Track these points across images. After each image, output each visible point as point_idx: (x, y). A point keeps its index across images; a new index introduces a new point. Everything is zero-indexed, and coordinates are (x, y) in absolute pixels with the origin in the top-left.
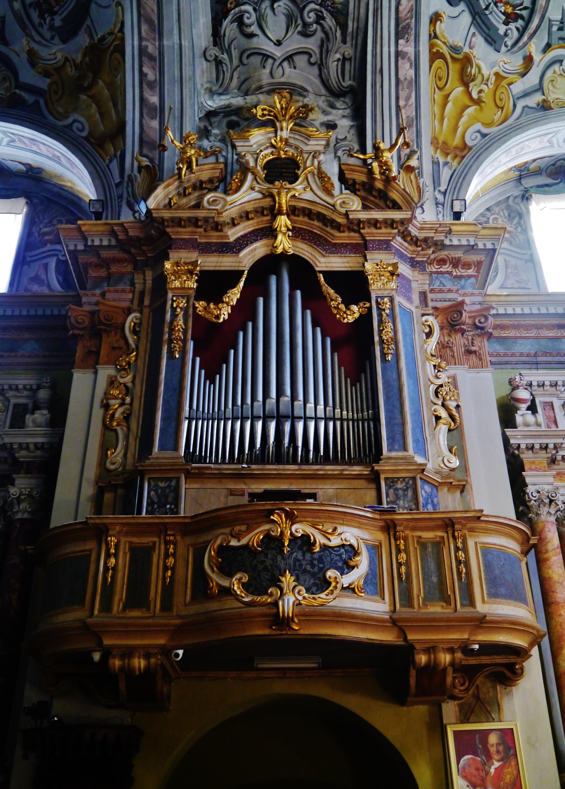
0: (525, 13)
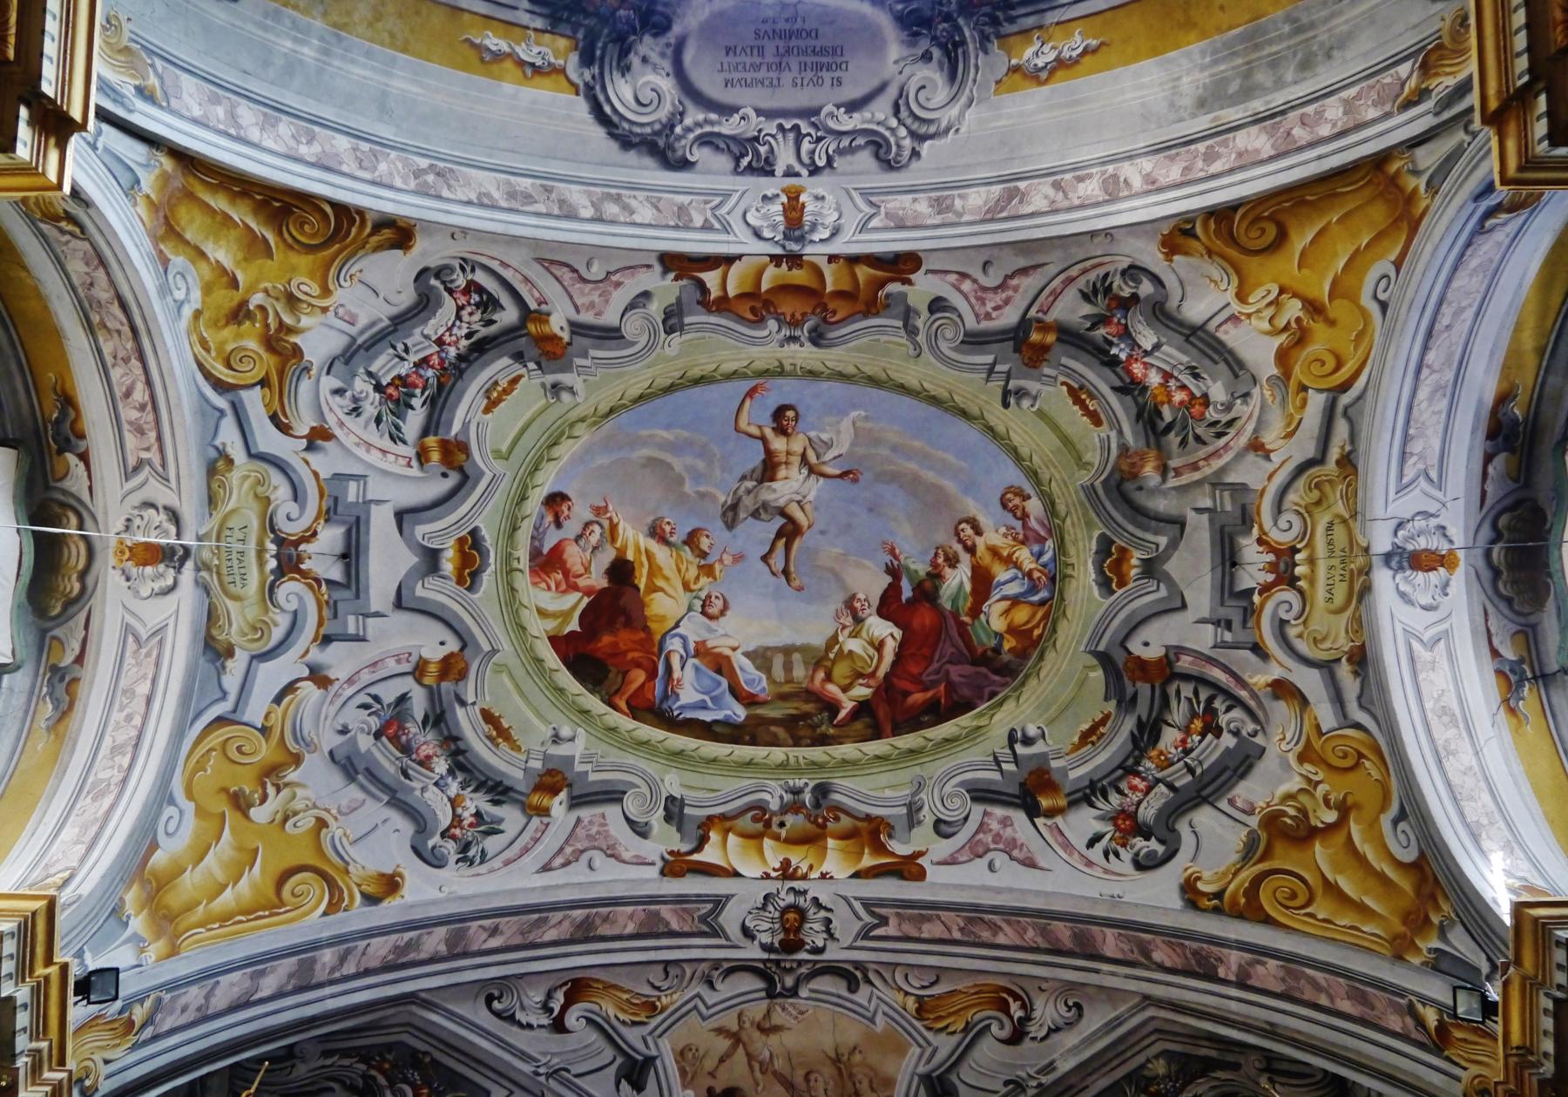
0: (1204, 694)
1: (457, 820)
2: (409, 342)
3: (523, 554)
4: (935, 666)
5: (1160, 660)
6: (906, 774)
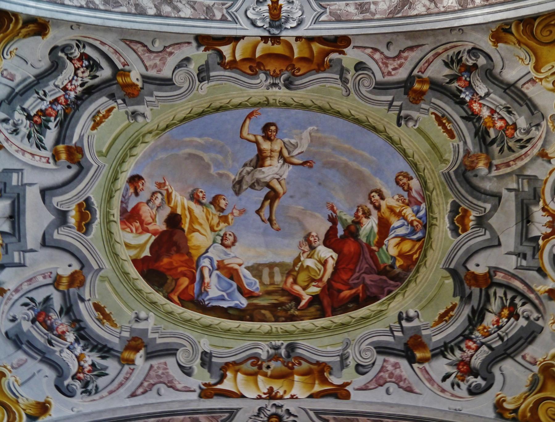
0: (509, 296)
1: (81, 368)
2: (47, 90)
3: (116, 212)
4: (357, 275)
5: (485, 274)
6: (340, 338)
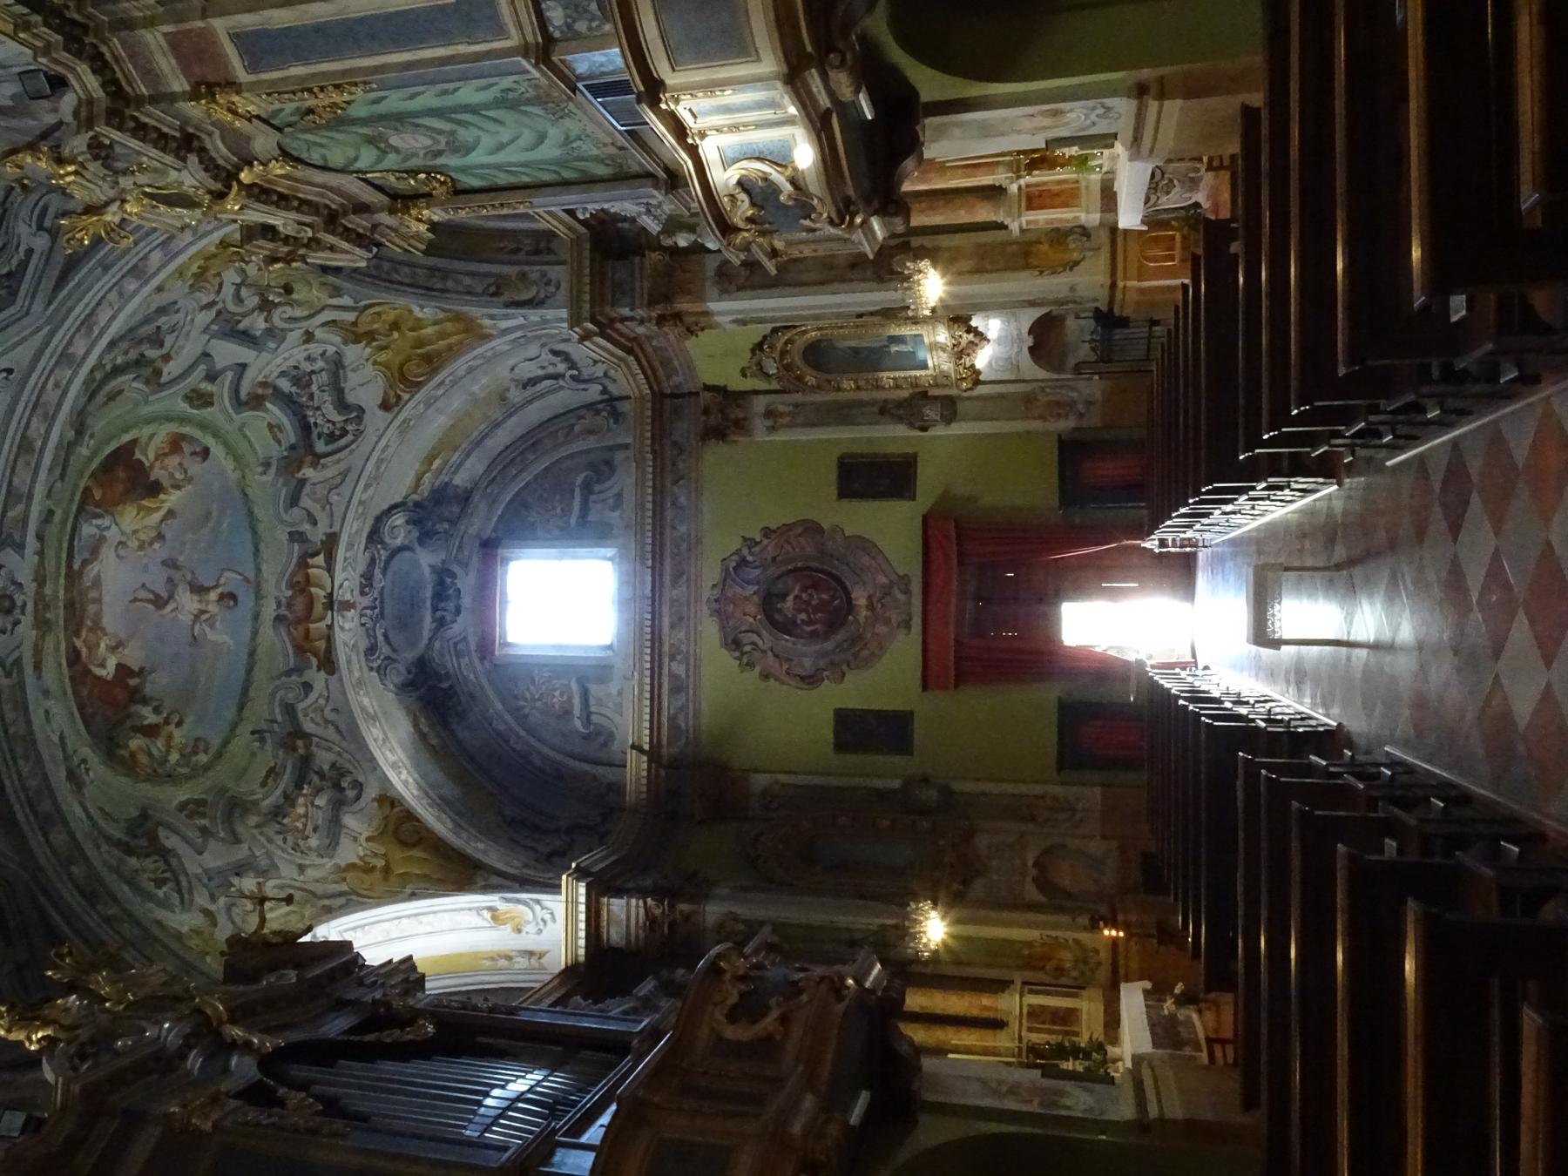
3: (187, 430)
